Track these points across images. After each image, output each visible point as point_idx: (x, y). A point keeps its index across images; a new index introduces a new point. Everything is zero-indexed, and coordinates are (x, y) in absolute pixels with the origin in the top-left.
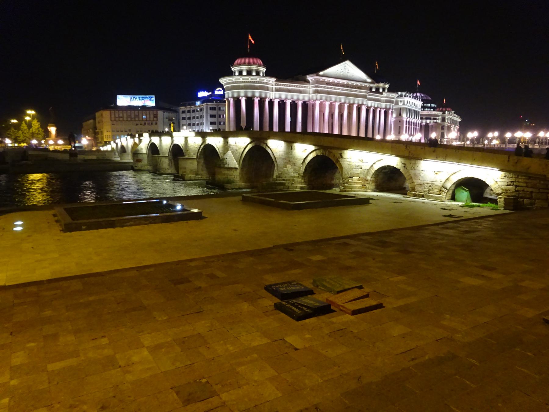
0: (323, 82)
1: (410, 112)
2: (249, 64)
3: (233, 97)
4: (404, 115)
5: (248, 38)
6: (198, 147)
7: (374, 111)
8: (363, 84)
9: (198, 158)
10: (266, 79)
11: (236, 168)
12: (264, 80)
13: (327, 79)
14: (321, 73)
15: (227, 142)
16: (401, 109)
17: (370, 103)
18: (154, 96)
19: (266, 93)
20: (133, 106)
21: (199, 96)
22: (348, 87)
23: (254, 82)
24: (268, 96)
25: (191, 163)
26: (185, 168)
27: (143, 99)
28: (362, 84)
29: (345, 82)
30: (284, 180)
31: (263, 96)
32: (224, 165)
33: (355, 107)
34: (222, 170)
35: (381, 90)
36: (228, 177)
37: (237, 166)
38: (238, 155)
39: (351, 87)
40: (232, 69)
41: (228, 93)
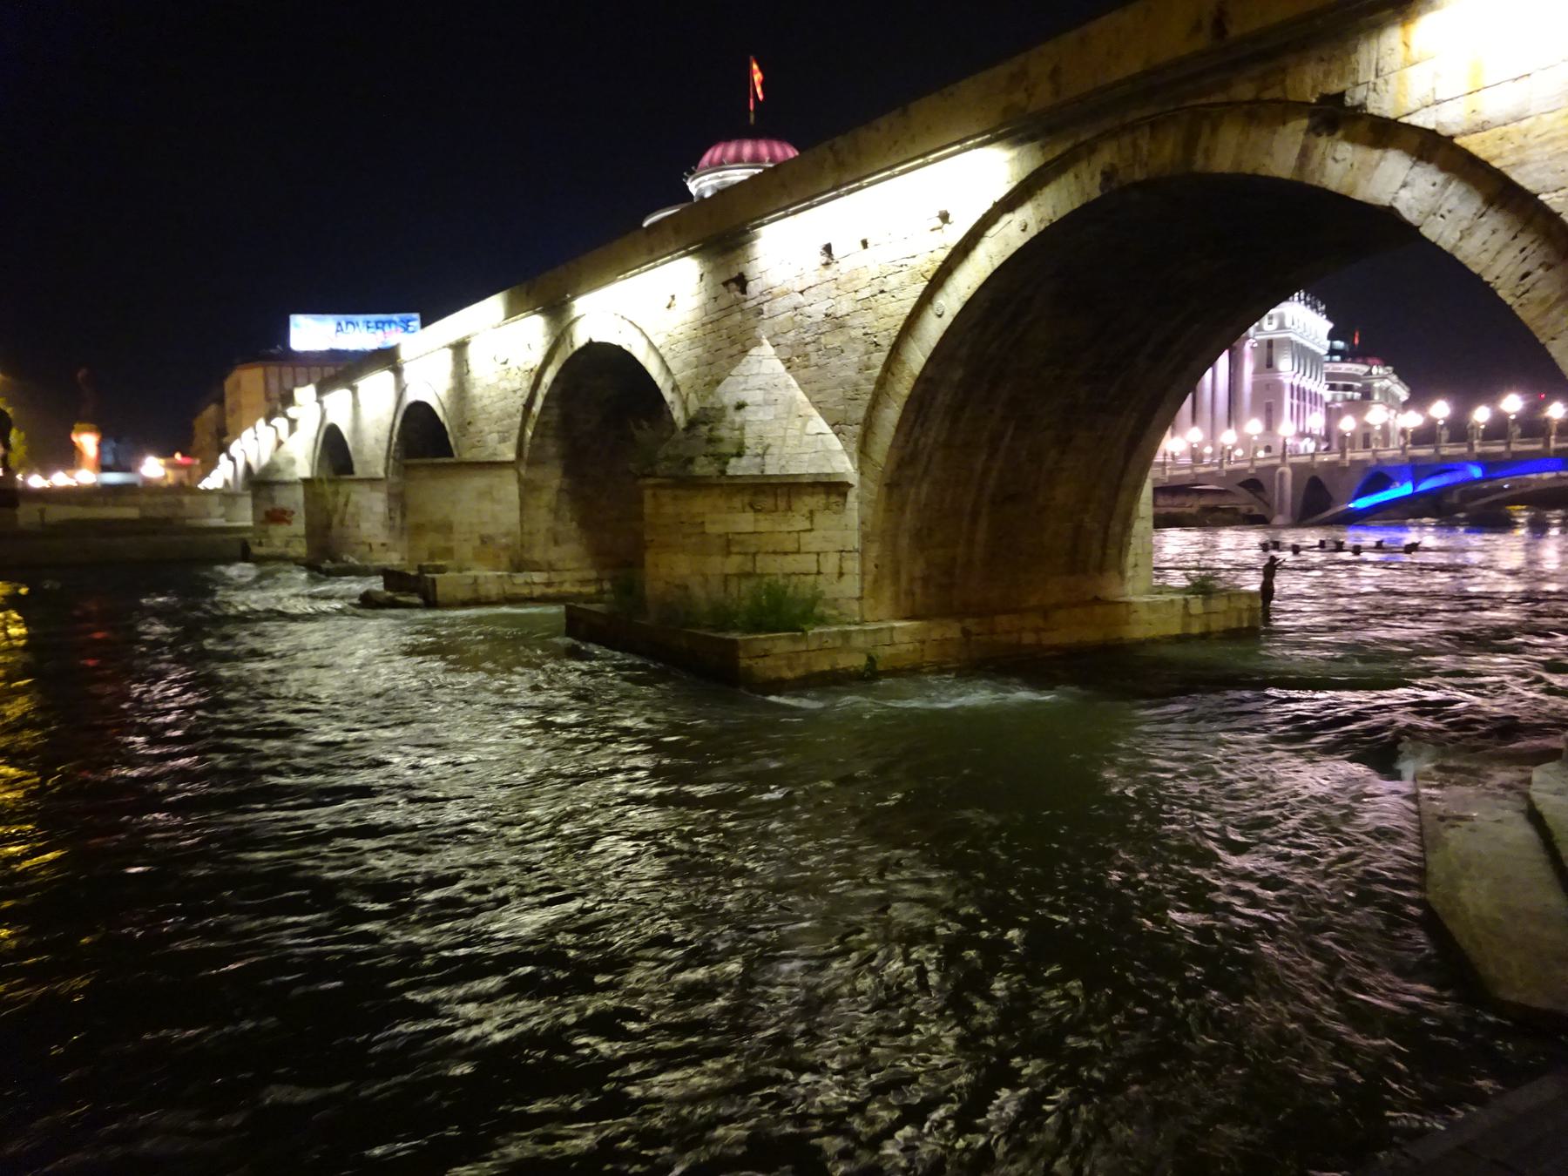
4: (1285, 364)
5: (749, 73)
6: (525, 385)
9: (528, 456)
11: (834, 488)
15: (741, 282)
16: (1270, 343)
18: (416, 316)
20: (346, 352)
25: (485, 494)
26: (446, 528)
27: (379, 325)
32: (723, 459)
34: (700, 505)
36: (773, 566)
37: (844, 465)
38: (853, 366)
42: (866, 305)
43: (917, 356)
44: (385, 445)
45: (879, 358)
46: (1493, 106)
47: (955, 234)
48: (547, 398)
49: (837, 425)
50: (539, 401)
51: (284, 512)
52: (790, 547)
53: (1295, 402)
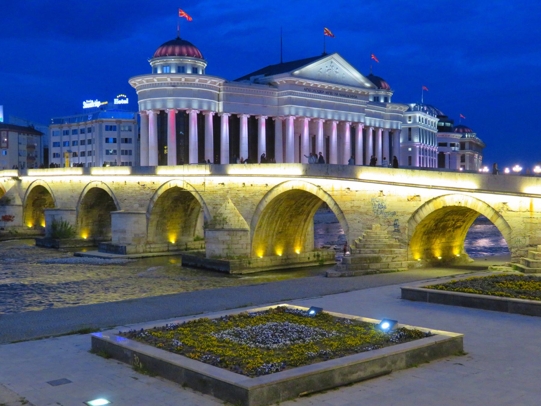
0: (300, 87)
1: (423, 133)
2: (181, 54)
3: (154, 109)
7: (375, 133)
8: (360, 91)
10: (210, 81)
11: (245, 231)
12: (206, 81)
13: (305, 82)
14: (297, 72)
16: (410, 129)
17: (368, 121)
19: (209, 104)
21: (84, 107)
22: (336, 94)
23: (191, 85)
24: (213, 109)
25: (137, 222)
28: (358, 90)
29: (333, 87)
30: (374, 252)
31: (205, 108)
33: (348, 125)
34: (217, 234)
35: (382, 101)
37: (247, 227)
39: (341, 95)
40: (151, 64)
41: (145, 103)
42: (252, 197)
43: (262, 208)
44: (78, 199)
45: (255, 207)
46: (335, 193)
47: (269, 188)
48: (159, 198)
49: (246, 219)
50: (156, 198)
51: (10, 217)
52: (236, 242)
53: (422, 156)
